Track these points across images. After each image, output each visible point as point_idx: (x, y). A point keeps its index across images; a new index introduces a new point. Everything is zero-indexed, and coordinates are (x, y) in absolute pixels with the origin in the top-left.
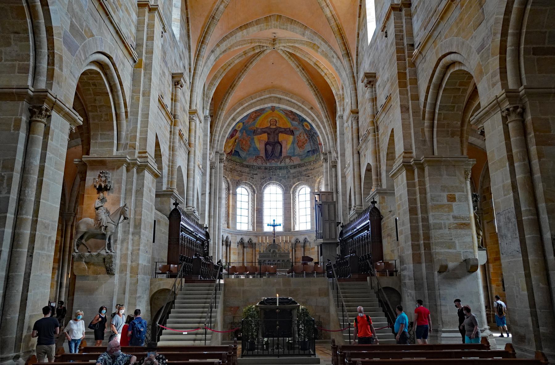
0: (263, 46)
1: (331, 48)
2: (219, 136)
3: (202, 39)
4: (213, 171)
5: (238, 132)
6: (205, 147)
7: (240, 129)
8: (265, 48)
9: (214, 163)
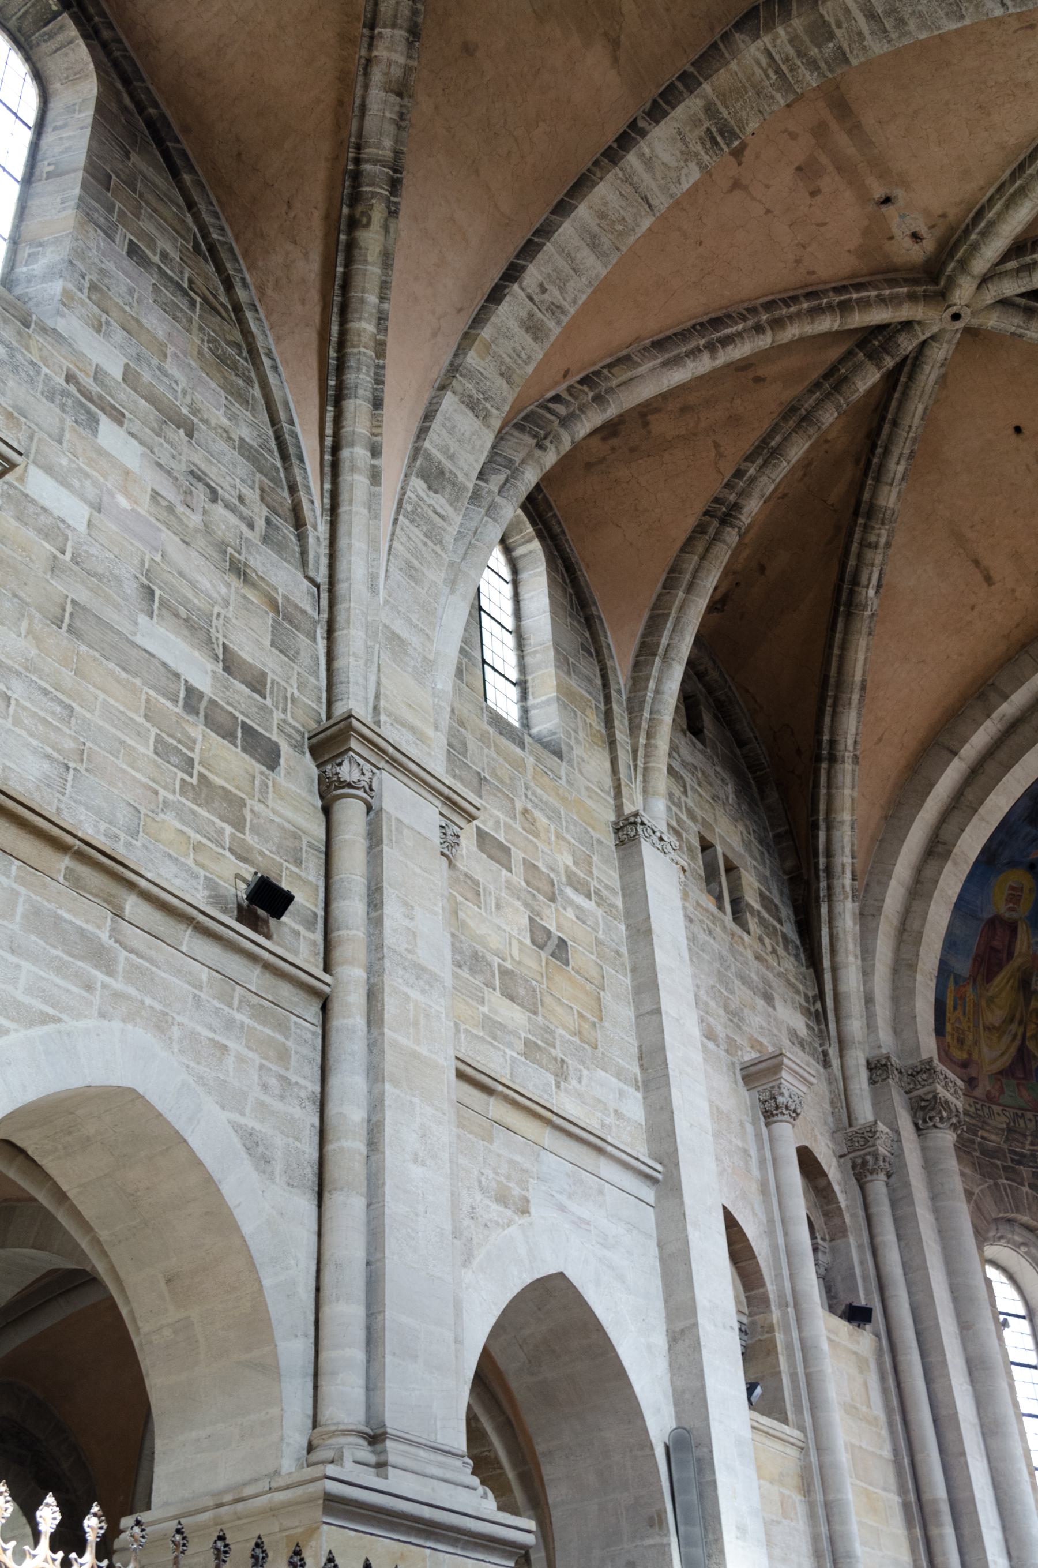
2: (867, 973)
3: (335, 329)
4: (879, 1187)
5: (1022, 930)
6: (648, 1006)
7: (1025, 908)
8: (907, 345)
9: (870, 1133)
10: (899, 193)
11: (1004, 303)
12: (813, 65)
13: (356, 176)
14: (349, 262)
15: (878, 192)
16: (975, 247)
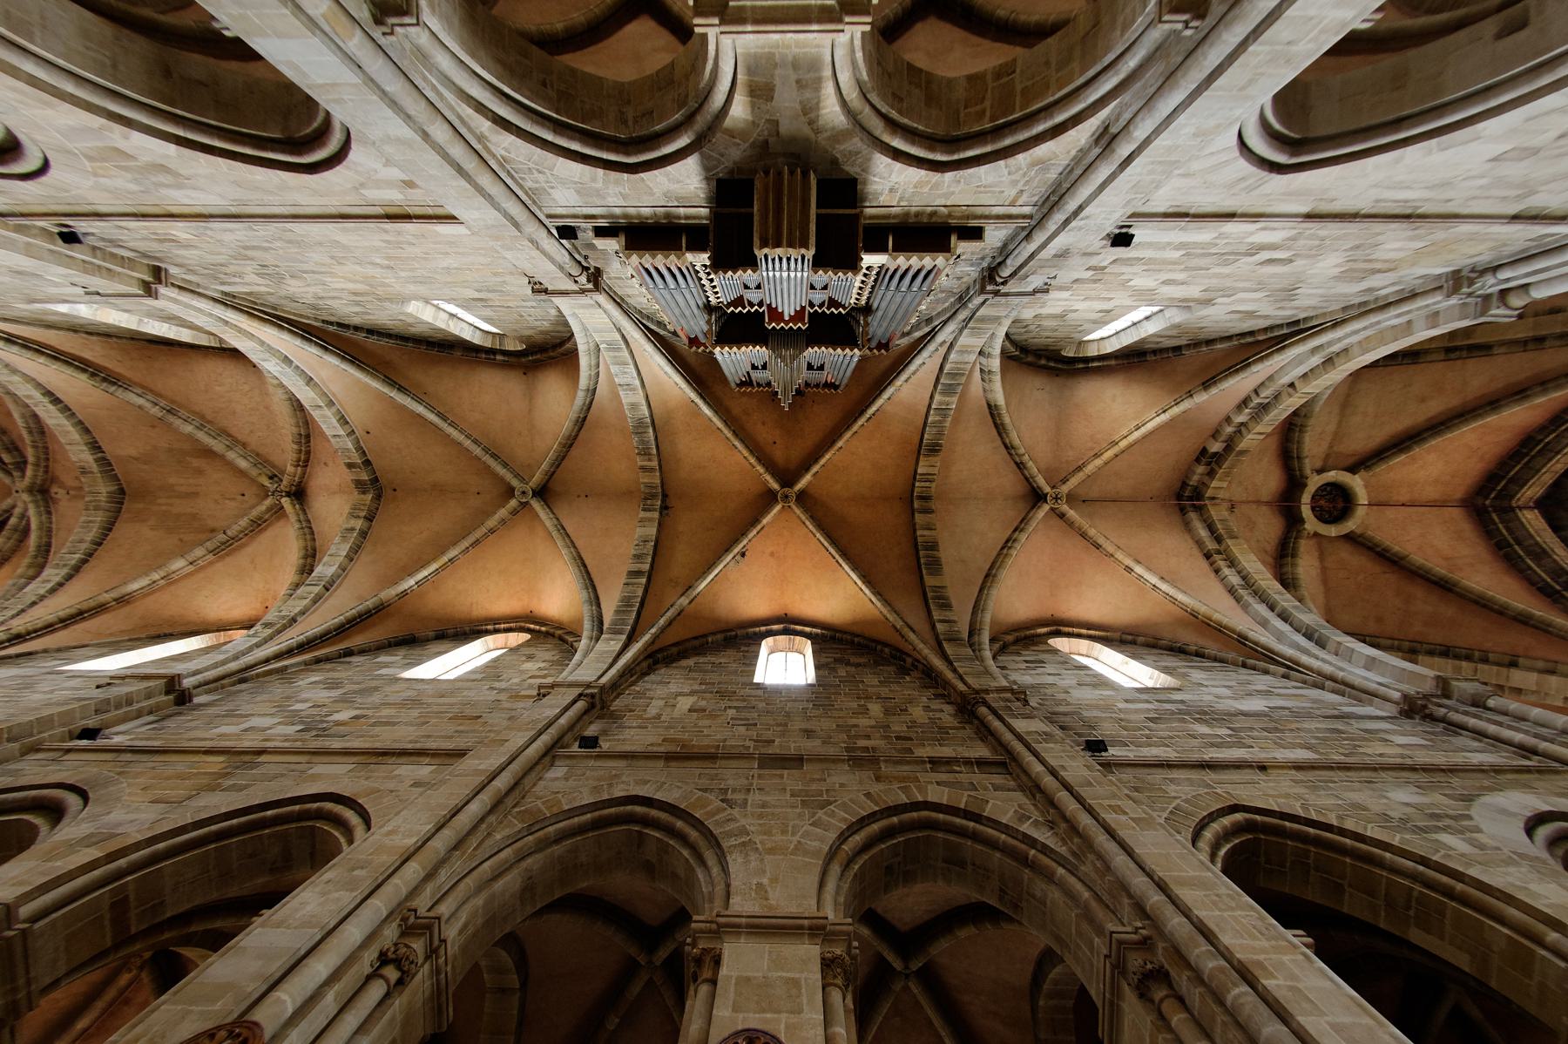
0: (23, 471)
1: (34, 604)
10: (68, 497)
11: (14, 507)
12: (91, 502)
13: (114, 384)
14: (77, 367)
15: (71, 492)
16: (38, 507)
